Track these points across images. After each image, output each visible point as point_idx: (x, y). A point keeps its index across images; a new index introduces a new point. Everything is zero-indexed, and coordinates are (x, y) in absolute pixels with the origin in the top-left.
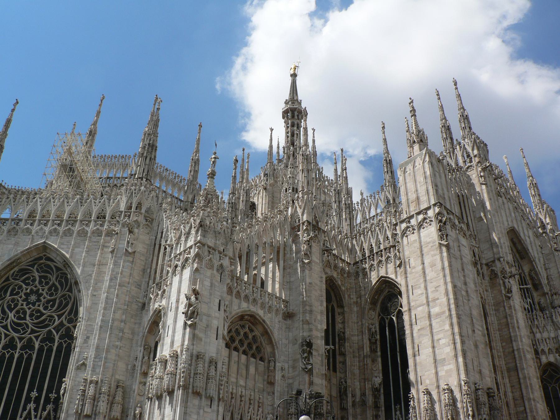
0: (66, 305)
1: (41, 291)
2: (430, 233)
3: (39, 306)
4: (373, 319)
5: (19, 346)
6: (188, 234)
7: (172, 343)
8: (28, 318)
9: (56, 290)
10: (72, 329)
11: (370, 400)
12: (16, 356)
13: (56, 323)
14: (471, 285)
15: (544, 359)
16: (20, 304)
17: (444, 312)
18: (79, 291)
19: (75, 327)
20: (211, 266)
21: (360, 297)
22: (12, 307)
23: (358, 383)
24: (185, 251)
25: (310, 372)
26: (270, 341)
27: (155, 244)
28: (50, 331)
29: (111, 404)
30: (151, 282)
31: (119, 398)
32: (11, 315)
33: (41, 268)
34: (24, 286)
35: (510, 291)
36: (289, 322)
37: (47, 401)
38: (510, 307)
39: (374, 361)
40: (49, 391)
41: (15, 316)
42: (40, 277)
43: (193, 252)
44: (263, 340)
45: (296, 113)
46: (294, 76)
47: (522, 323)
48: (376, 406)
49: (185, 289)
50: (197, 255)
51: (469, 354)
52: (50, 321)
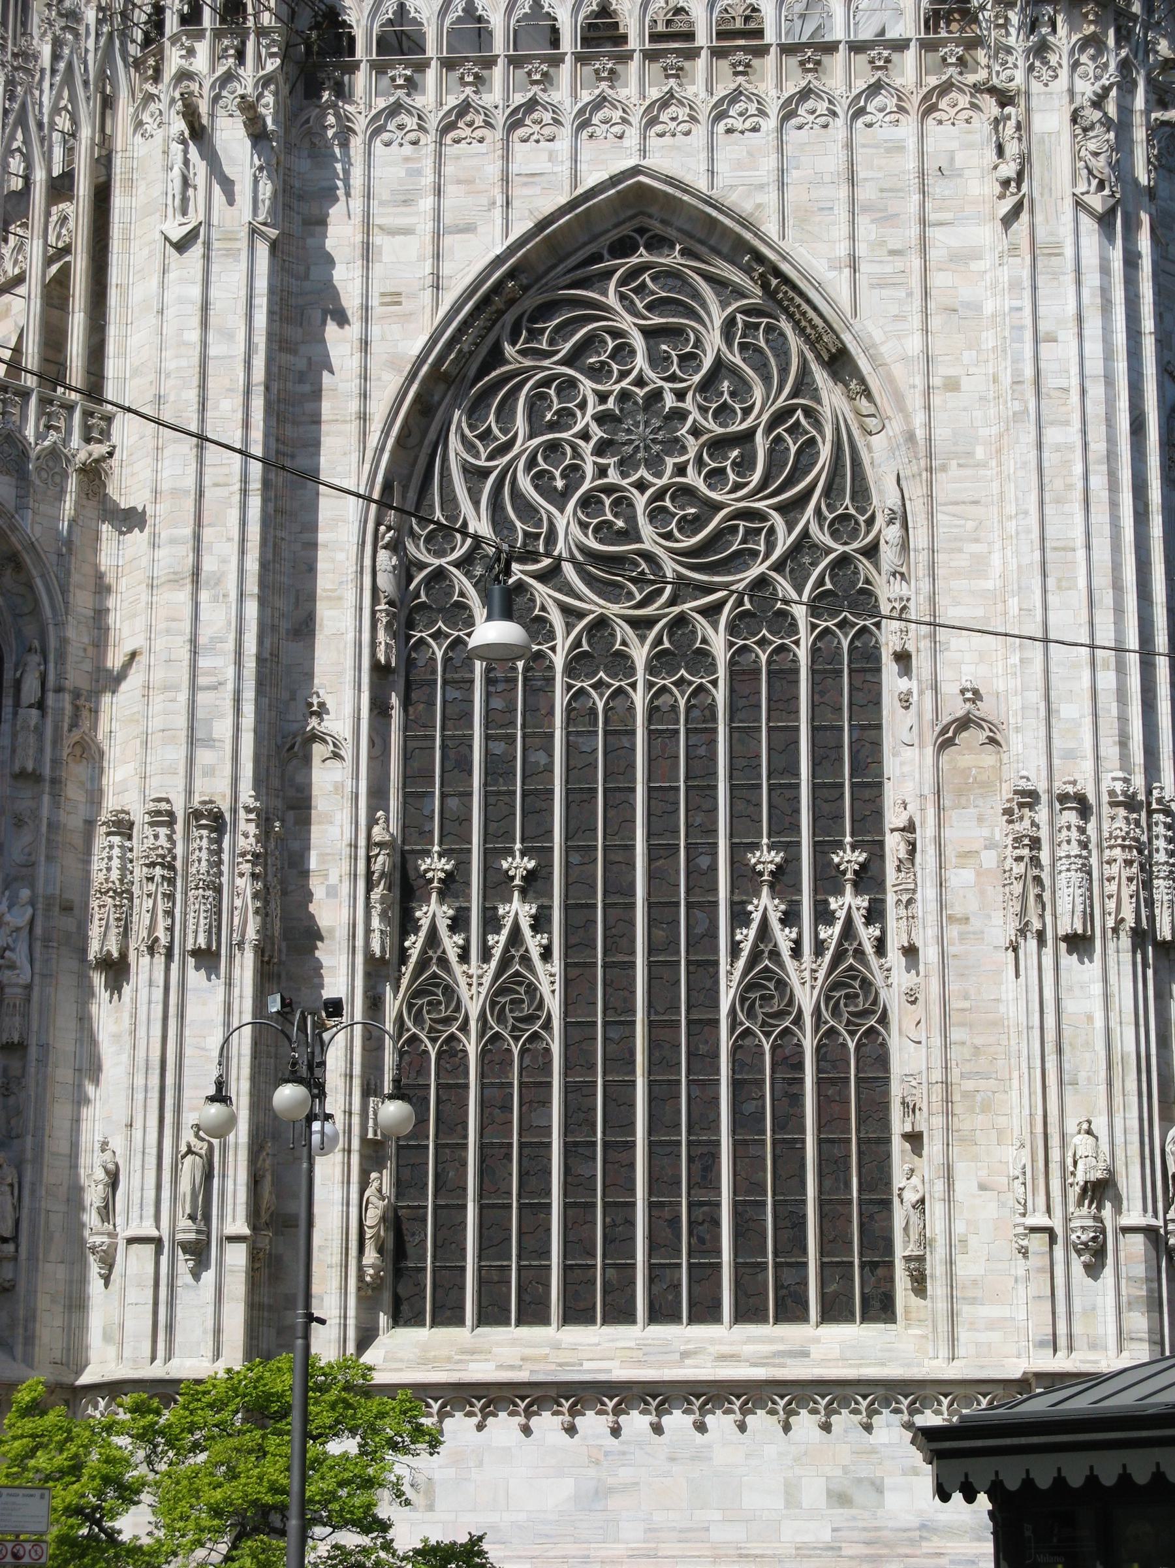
1: (670, 401)
3: (681, 470)
5: (640, 654)
8: (646, 529)
9: (742, 389)
10: (864, 565)
12: (639, 699)
13: (784, 541)
16: (589, 470)
22: (560, 484)
28: (762, 582)
32: (565, 521)
33: (641, 289)
34: (587, 386)
41: (584, 526)
42: (647, 332)
52: (752, 533)
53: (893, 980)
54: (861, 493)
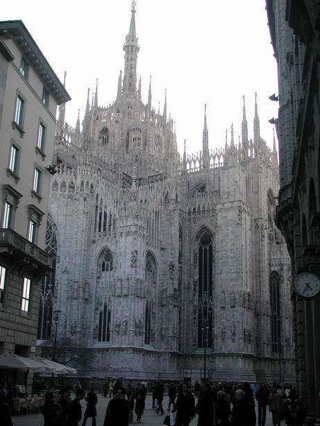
0: (50, 237)
2: (233, 215)
4: (196, 246)
6: (127, 217)
7: (124, 272)
11: (192, 287)
14: (248, 242)
15: (273, 269)
17: (235, 257)
18: (57, 229)
19: (56, 249)
20: (140, 236)
21: (191, 233)
23: (186, 278)
24: (127, 226)
25: (173, 279)
26: (155, 263)
27: (97, 207)
29: (84, 292)
30: (97, 230)
31: (87, 289)
35: (263, 237)
36: (162, 252)
37: (48, 288)
38: (262, 246)
39: (195, 267)
40: (48, 283)
43: (133, 229)
44: (152, 262)
45: (134, 49)
46: (133, 12)
47: (266, 253)
48: (195, 290)
49: (130, 249)
50: (136, 231)
51: (244, 278)
53: (53, 299)
54: (56, 242)
